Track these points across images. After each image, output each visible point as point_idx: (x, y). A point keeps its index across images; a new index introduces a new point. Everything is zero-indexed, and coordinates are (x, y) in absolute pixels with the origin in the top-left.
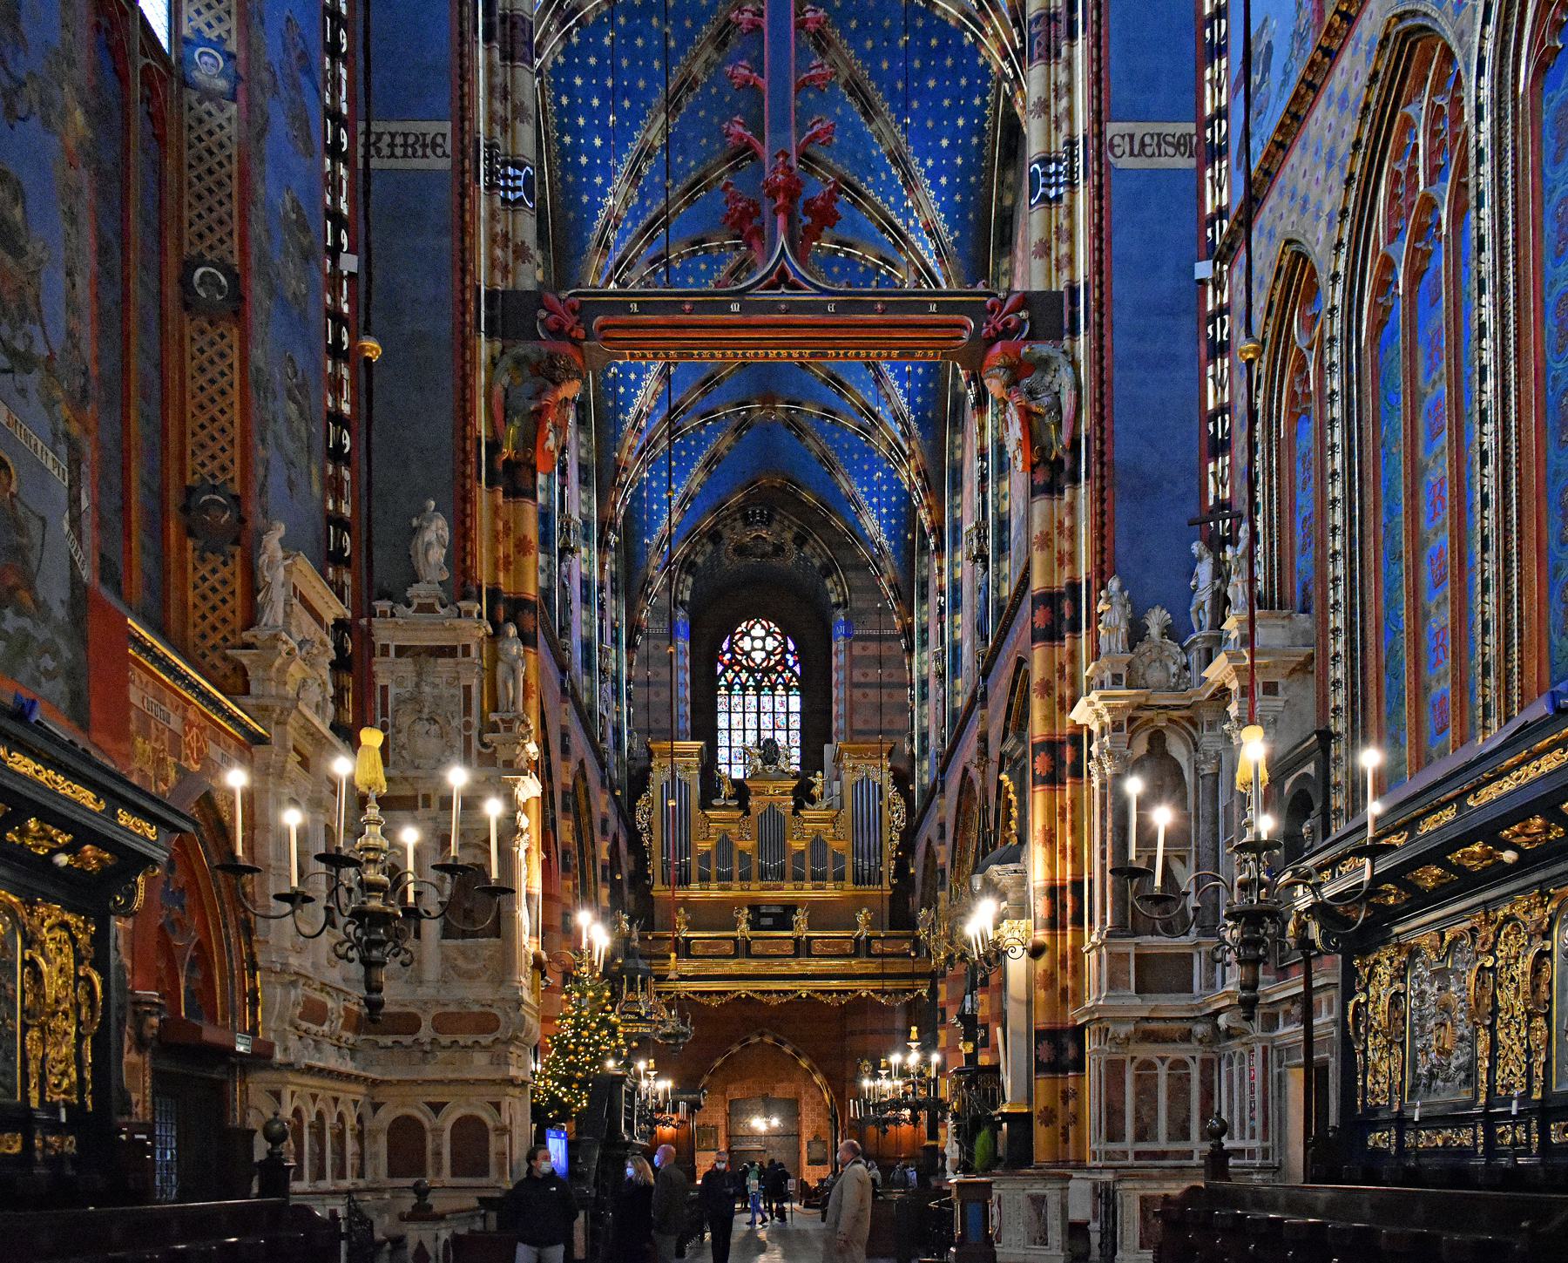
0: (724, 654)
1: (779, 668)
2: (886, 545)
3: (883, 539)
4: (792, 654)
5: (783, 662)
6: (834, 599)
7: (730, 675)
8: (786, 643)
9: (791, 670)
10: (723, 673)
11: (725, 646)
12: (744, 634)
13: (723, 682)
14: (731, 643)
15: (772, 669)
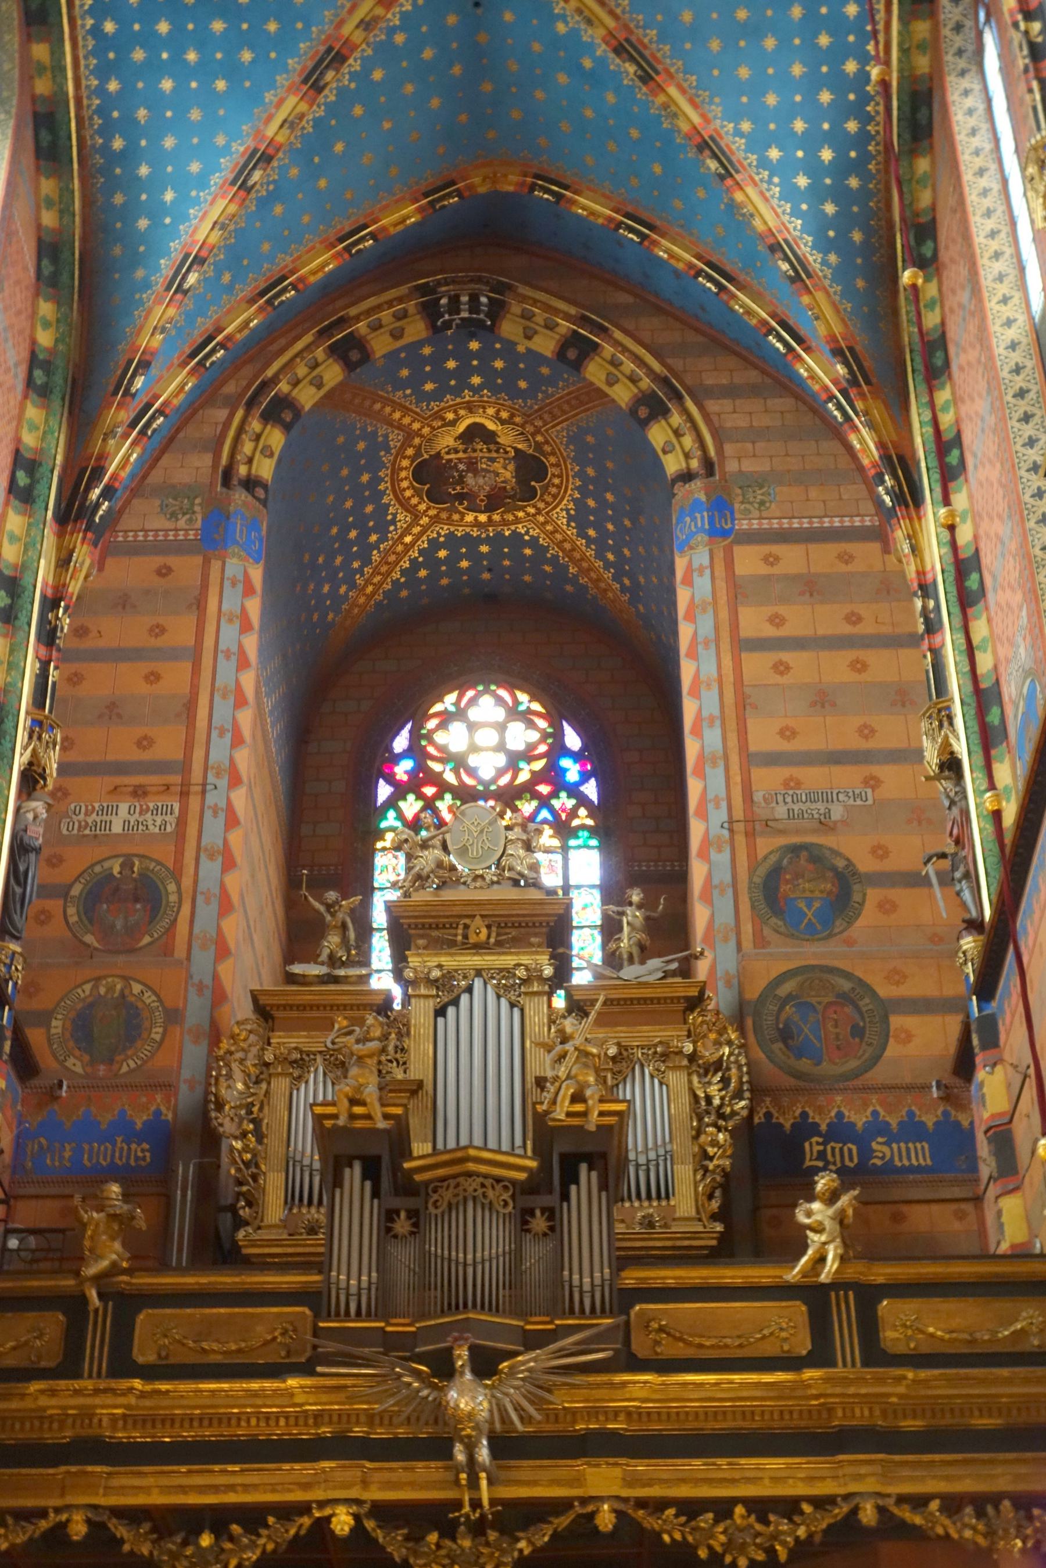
0: (397, 758)
1: (544, 789)
2: (814, 259)
3: (806, 248)
4: (577, 756)
5: (553, 775)
6: (672, 464)
7: (411, 806)
8: (558, 735)
9: (573, 791)
10: (392, 802)
11: (401, 743)
12: (446, 719)
13: (390, 820)
14: (415, 736)
15: (528, 790)
